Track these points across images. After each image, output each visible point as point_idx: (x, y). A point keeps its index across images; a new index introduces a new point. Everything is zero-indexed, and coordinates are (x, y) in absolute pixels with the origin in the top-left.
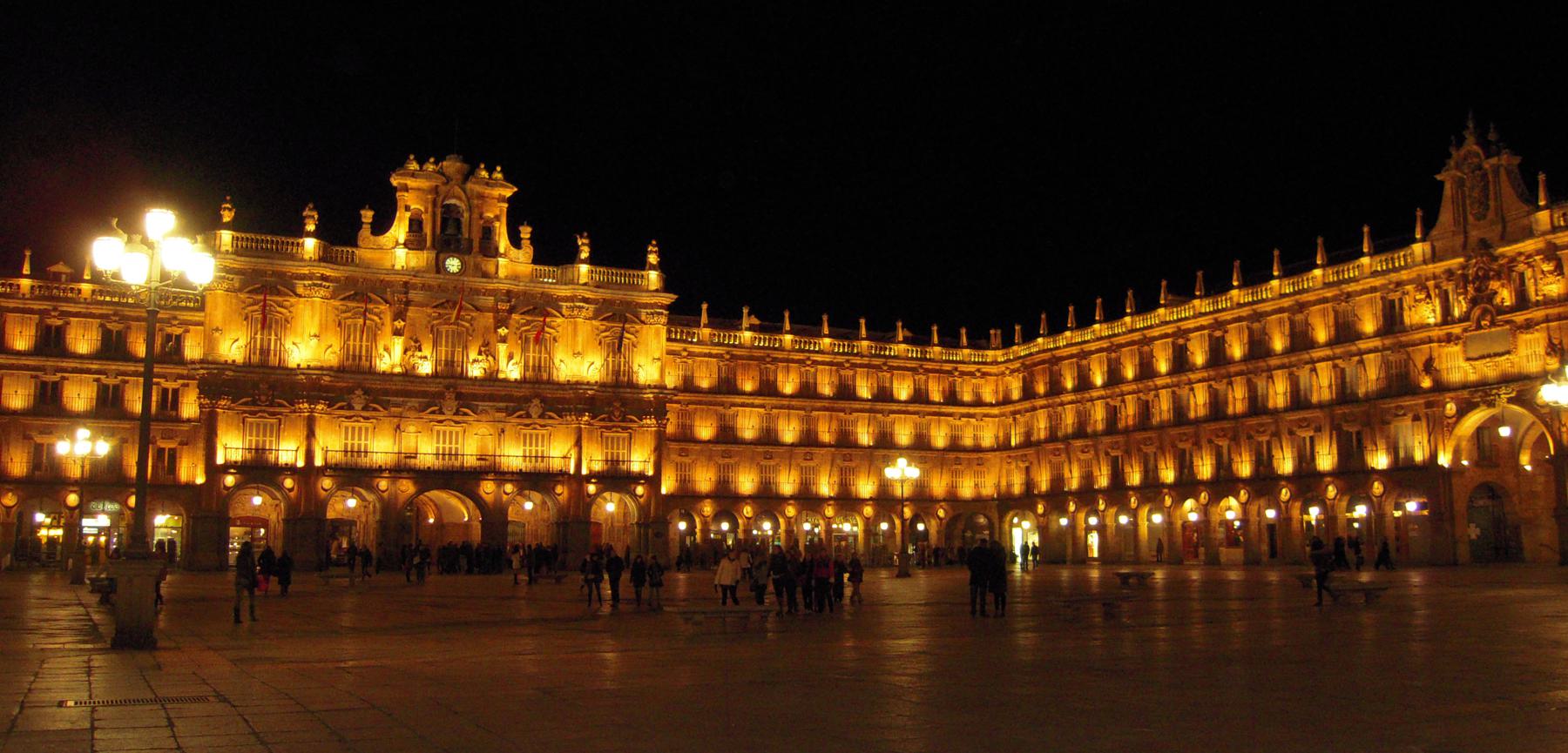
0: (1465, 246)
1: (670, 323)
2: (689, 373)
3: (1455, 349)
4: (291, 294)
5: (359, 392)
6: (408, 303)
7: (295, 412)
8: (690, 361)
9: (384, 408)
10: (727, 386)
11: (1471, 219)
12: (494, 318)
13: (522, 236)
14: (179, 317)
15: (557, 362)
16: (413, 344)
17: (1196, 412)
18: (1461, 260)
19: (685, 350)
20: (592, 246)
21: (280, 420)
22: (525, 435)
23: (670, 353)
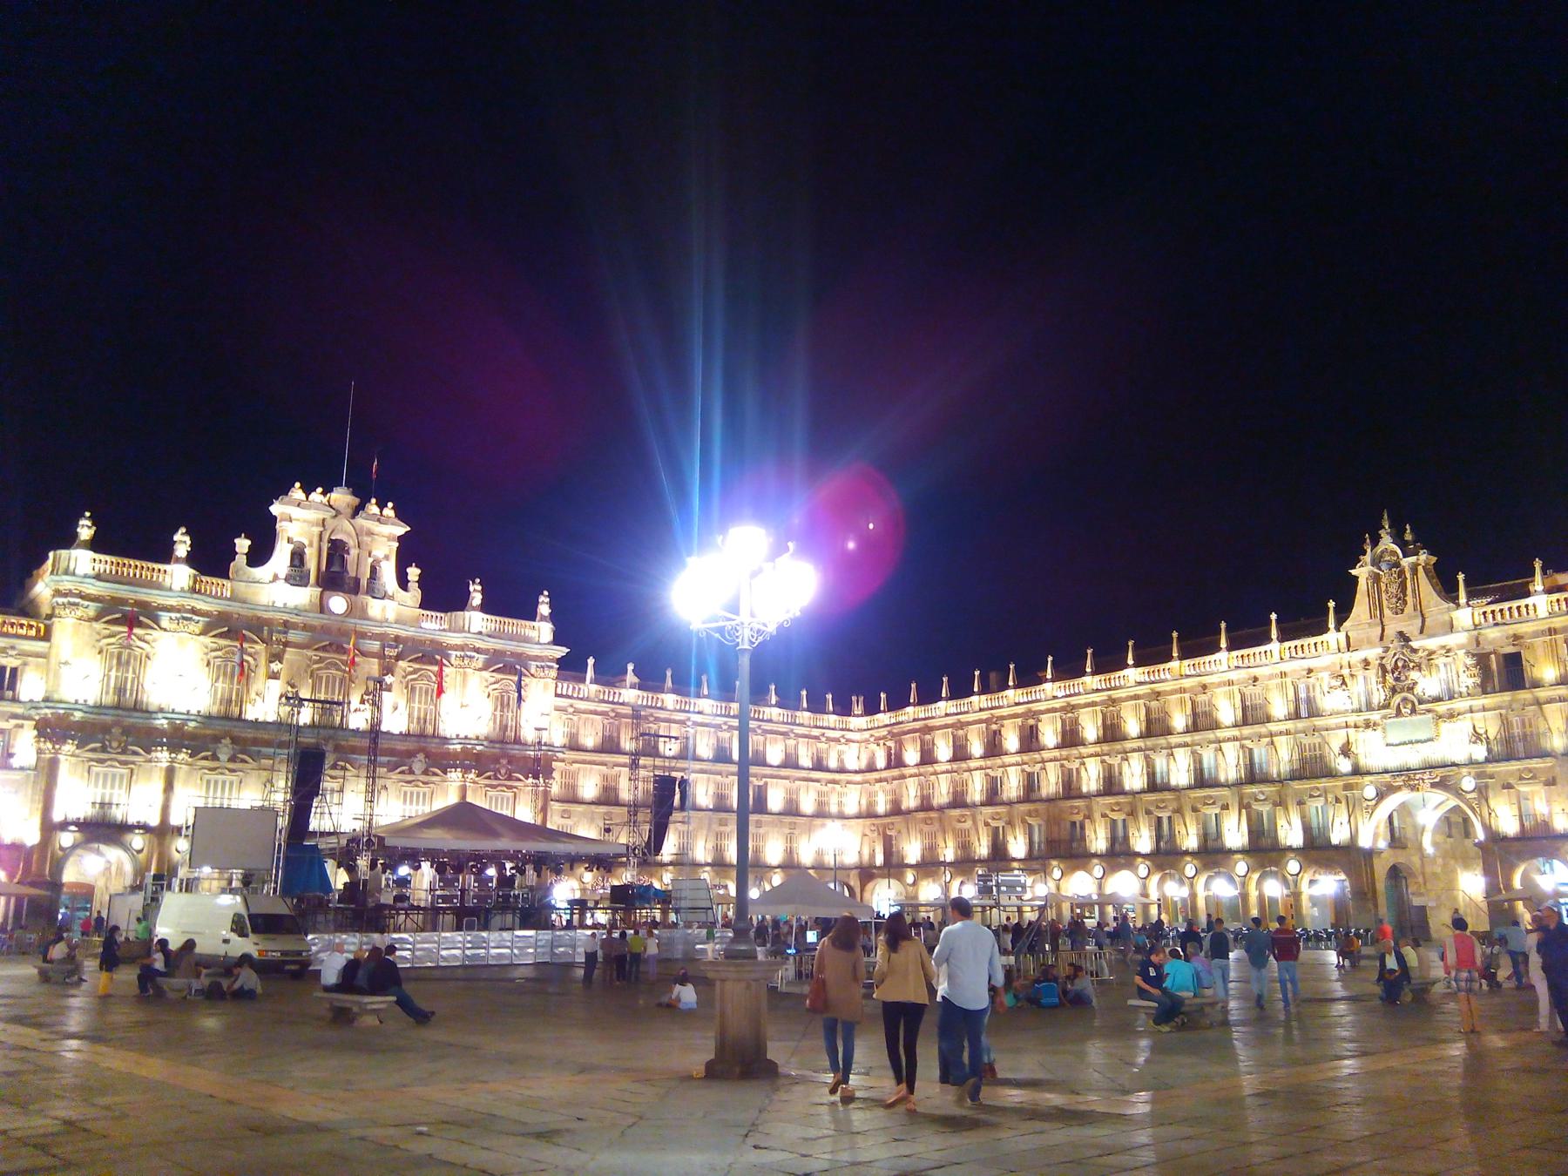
1: (557, 678)
2: (574, 731)
4: (156, 626)
5: (227, 741)
6: (286, 644)
7: (150, 761)
8: (575, 718)
10: (609, 746)
11: (1387, 612)
12: (379, 664)
13: (409, 578)
14: (17, 647)
16: (290, 689)
17: (1088, 785)
19: (571, 706)
20: (483, 592)
21: (132, 770)
22: (405, 793)
23: (557, 709)
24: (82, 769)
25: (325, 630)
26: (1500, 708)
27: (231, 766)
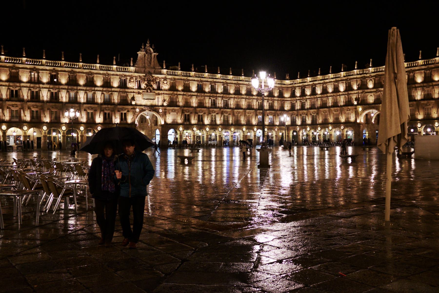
0: (144, 71)
3: (139, 95)
18: (144, 75)
26: (170, 94)
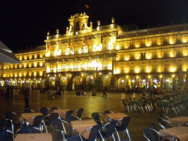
5: (63, 59)
6: (71, 42)
8: (123, 43)
9: (67, 61)
15: (94, 48)
19: (122, 40)
24: (49, 66)
25: (75, 38)
27: (65, 63)
